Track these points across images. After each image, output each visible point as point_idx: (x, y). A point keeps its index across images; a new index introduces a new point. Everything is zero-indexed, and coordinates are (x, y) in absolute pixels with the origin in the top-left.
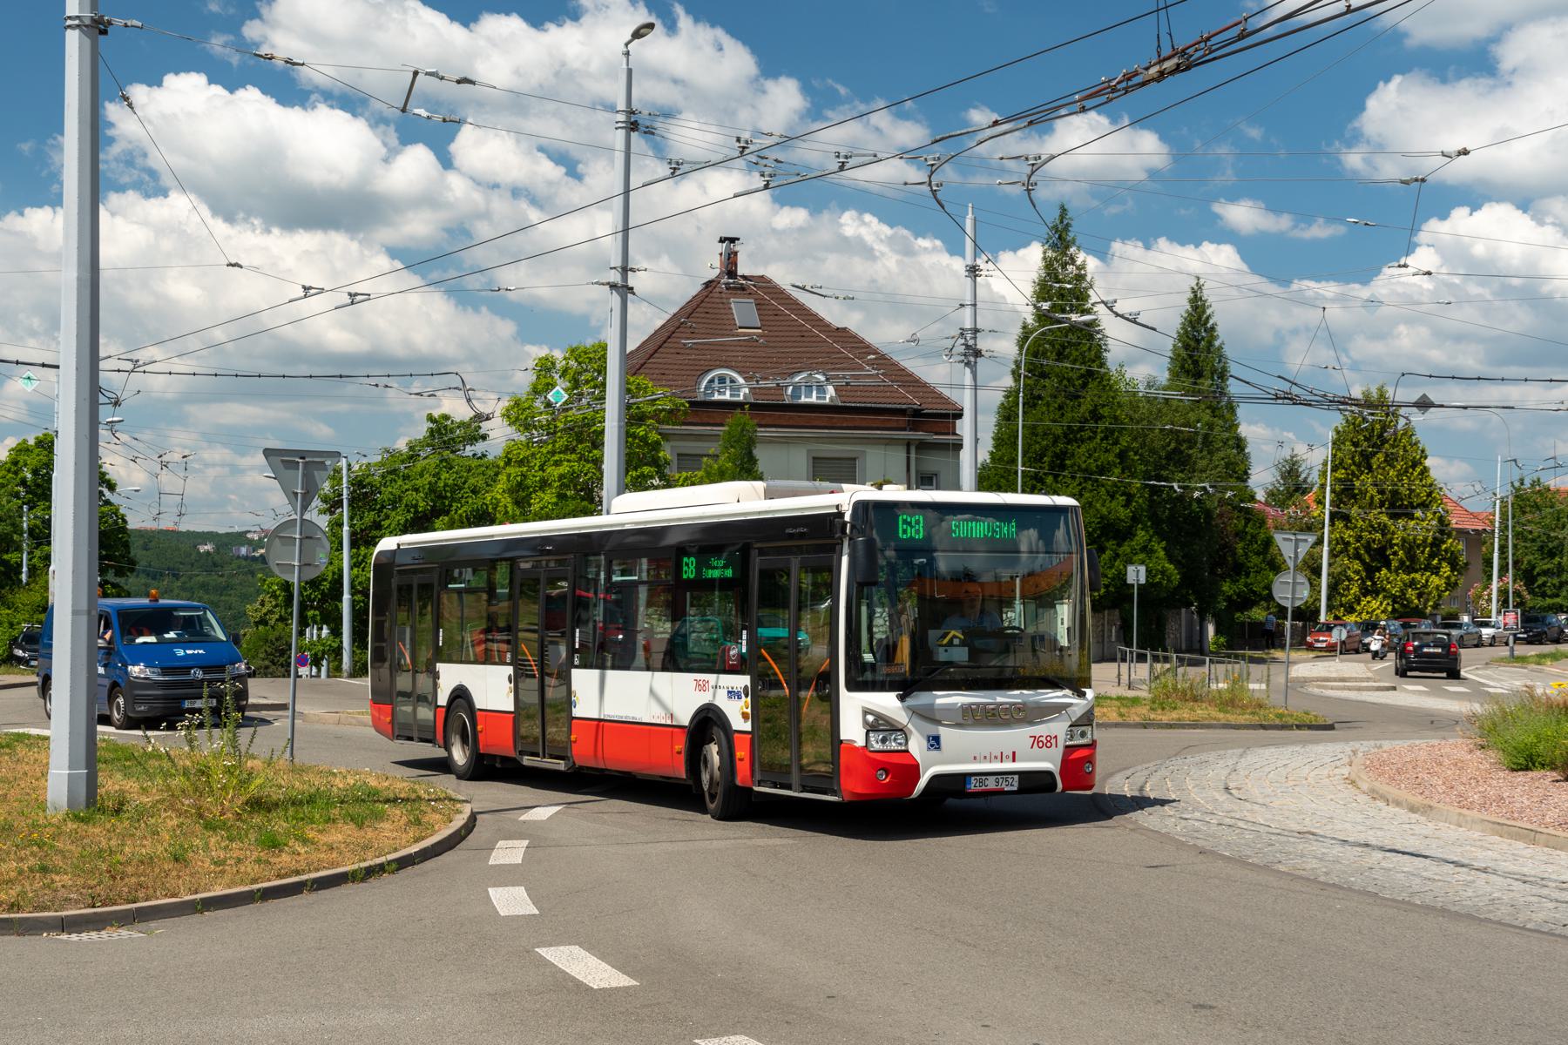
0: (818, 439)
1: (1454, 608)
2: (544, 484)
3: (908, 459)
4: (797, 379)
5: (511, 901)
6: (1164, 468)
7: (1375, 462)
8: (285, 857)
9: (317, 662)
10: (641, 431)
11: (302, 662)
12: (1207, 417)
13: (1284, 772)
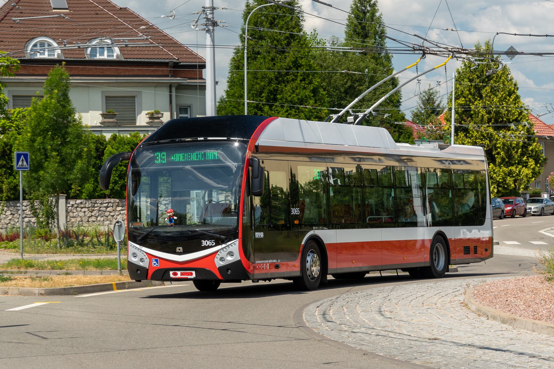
0: (109, 84)
1: (538, 189)
3: (171, 96)
4: (94, 43)
6: (342, 99)
12: (372, 65)
13: (421, 300)
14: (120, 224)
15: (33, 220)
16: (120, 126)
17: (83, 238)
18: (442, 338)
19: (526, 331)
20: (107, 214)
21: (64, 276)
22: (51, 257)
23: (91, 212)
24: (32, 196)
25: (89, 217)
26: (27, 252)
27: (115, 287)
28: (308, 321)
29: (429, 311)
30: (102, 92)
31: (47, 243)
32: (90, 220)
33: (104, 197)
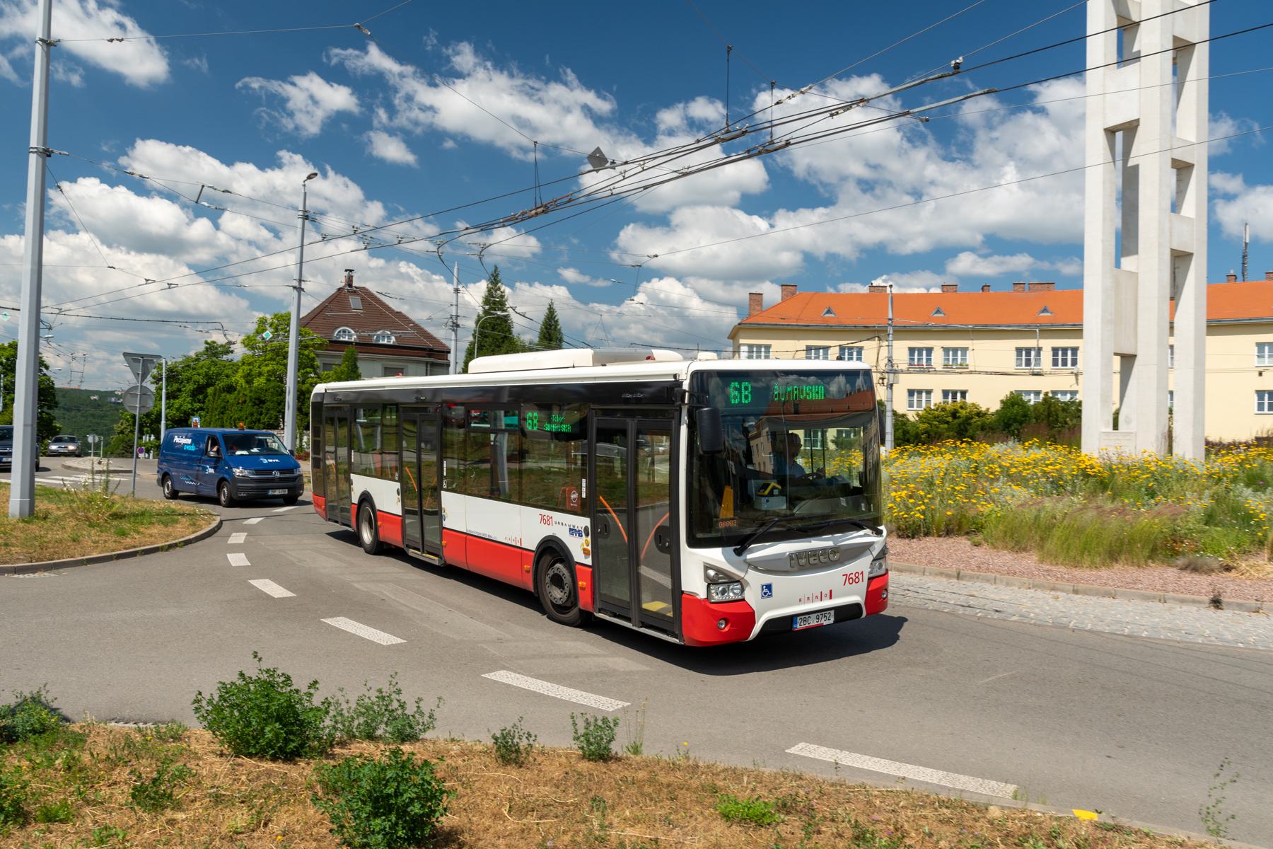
2: (260, 374)
5: (237, 560)
8: (128, 540)
9: (148, 451)
11: (141, 451)
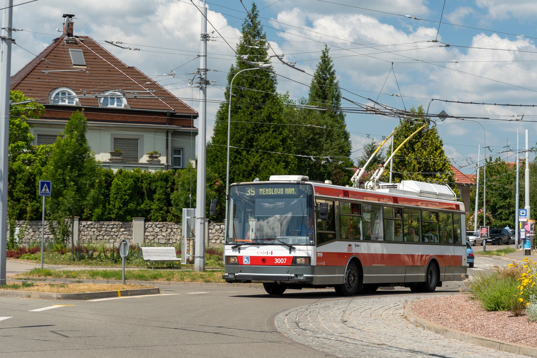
0: (117, 128)
3: (167, 140)
6: (306, 148)
7: (416, 147)
10: (17, 121)
13: (369, 312)
14: (125, 242)
15: (51, 236)
16: (125, 163)
17: (93, 253)
18: (388, 343)
19: (455, 340)
20: (112, 234)
21: (78, 284)
22: (66, 267)
23: (100, 232)
24: (51, 217)
25: (97, 236)
26: (46, 263)
27: (119, 294)
28: (279, 327)
29: (377, 321)
30: (112, 134)
31: (62, 256)
32: (98, 238)
33: (110, 219)
